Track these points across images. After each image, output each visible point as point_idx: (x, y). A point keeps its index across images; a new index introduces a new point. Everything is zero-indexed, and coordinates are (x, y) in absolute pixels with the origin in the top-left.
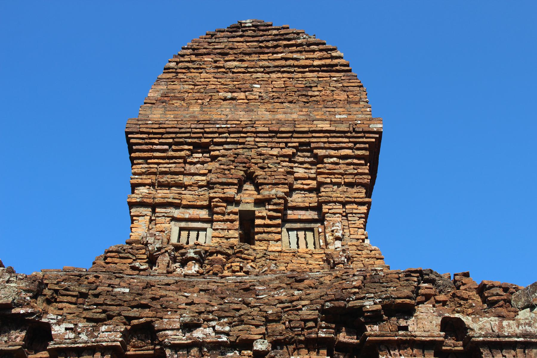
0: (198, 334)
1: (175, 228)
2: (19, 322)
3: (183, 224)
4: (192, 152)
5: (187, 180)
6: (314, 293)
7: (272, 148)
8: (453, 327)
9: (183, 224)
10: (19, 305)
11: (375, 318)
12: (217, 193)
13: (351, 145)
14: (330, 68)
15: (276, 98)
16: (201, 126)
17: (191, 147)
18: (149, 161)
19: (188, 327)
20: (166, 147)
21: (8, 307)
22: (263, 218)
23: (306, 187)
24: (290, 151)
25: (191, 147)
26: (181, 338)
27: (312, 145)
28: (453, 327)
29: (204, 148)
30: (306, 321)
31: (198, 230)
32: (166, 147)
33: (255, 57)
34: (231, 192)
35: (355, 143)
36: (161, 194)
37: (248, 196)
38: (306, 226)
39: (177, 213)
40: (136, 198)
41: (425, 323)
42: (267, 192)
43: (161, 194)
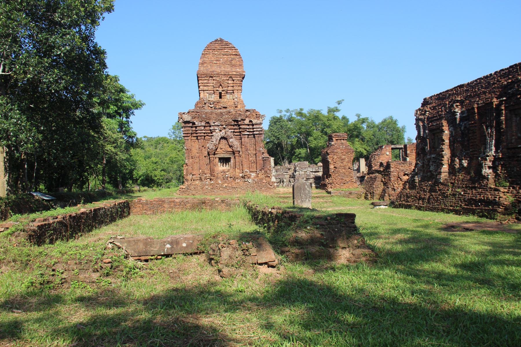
0: (215, 124)
1: (208, 95)
2: (191, 122)
6: (232, 116)
8: (251, 121)
11: (240, 121)
12: (215, 89)
14: (236, 55)
15: (224, 63)
19: (214, 123)
24: (228, 78)
26: (213, 124)
28: (251, 121)
29: (212, 77)
33: (221, 51)
34: (217, 89)
36: (206, 88)
37: (220, 89)
38: (231, 93)
39: (208, 92)
40: (200, 89)
41: (247, 121)
42: (224, 89)
43: (206, 88)
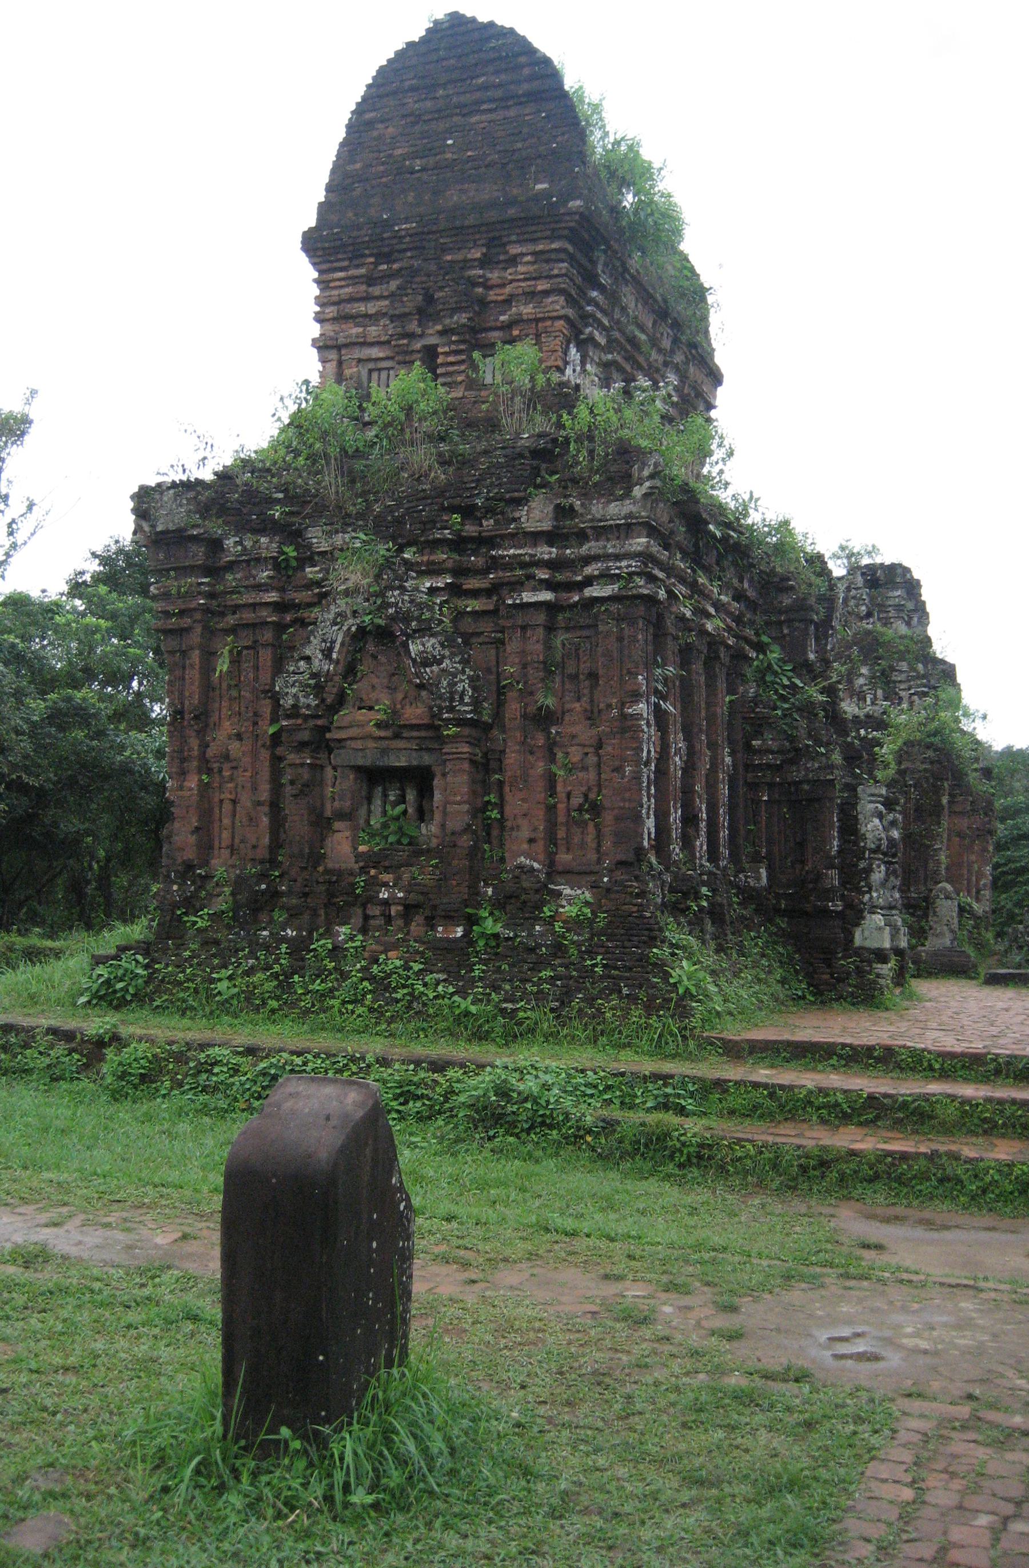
3: (371, 365)
4: (376, 264)
5: (372, 308)
7: (459, 249)
9: (371, 365)
10: (194, 526)
13: (549, 233)
16: (378, 231)
17: (372, 260)
18: (332, 285)
20: (346, 263)
21: (180, 531)
22: (446, 354)
23: (500, 298)
25: (372, 260)
27: (505, 240)
30: (424, 523)
31: (388, 369)
32: (346, 263)
35: (553, 230)
